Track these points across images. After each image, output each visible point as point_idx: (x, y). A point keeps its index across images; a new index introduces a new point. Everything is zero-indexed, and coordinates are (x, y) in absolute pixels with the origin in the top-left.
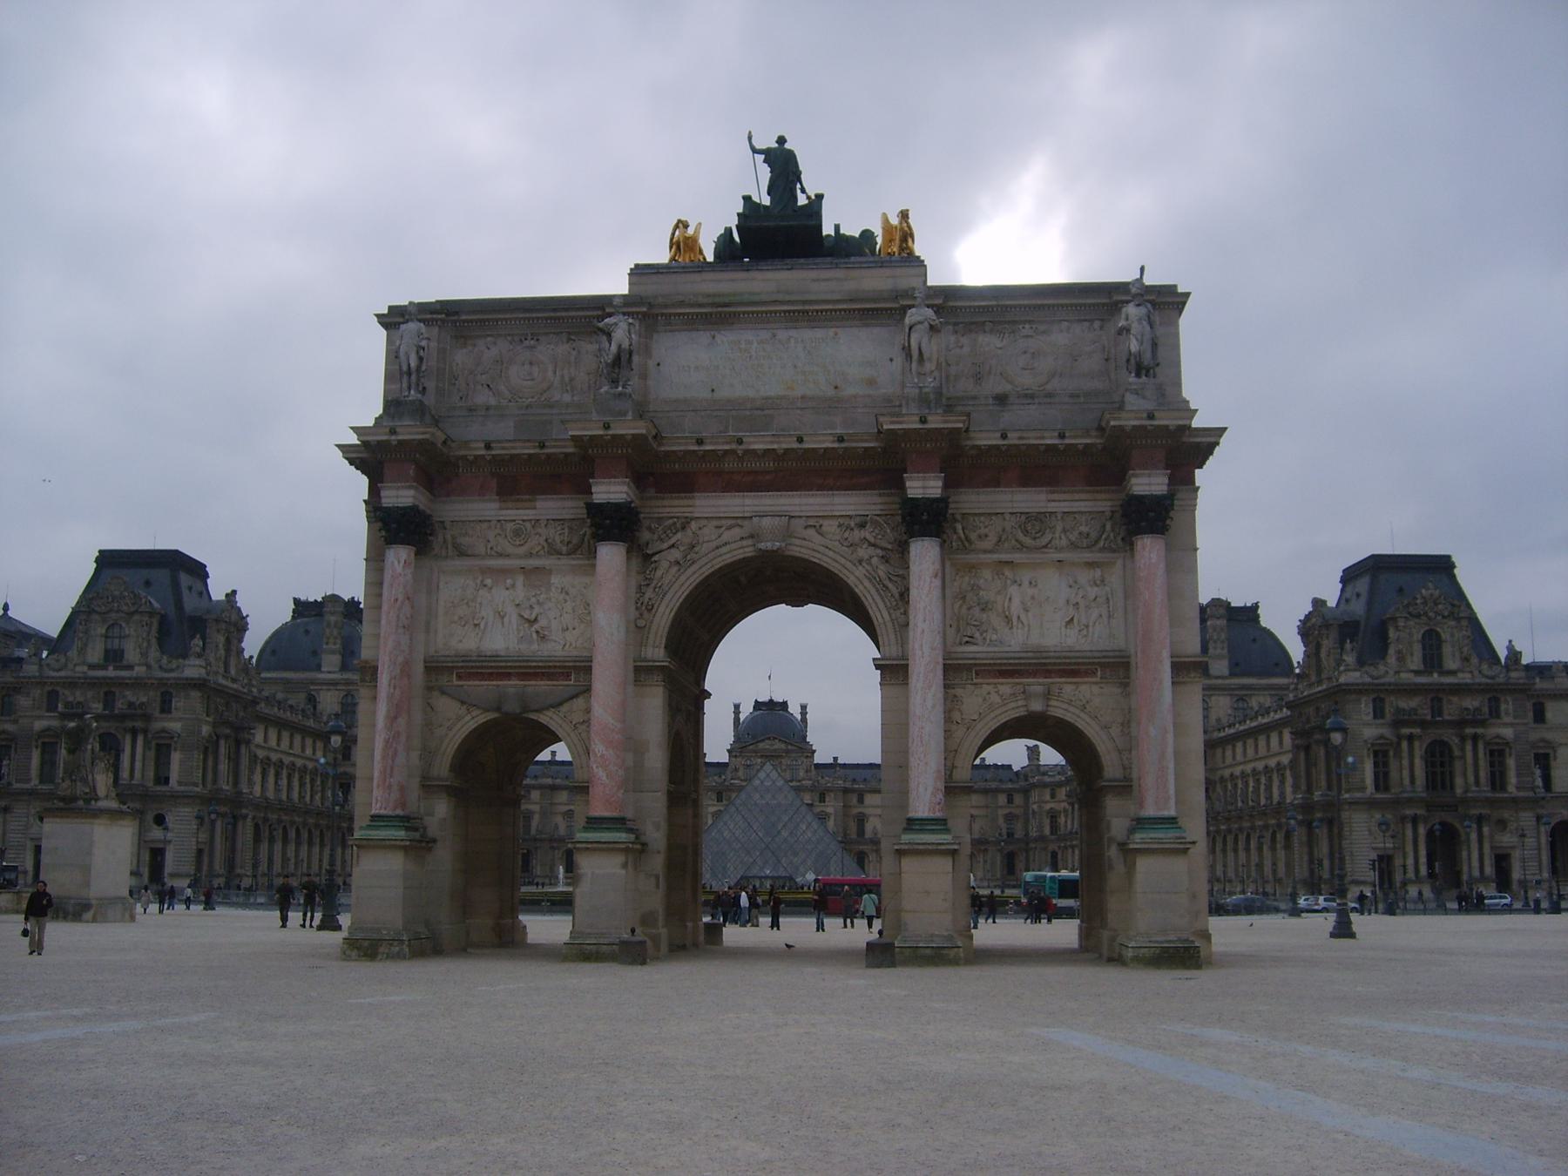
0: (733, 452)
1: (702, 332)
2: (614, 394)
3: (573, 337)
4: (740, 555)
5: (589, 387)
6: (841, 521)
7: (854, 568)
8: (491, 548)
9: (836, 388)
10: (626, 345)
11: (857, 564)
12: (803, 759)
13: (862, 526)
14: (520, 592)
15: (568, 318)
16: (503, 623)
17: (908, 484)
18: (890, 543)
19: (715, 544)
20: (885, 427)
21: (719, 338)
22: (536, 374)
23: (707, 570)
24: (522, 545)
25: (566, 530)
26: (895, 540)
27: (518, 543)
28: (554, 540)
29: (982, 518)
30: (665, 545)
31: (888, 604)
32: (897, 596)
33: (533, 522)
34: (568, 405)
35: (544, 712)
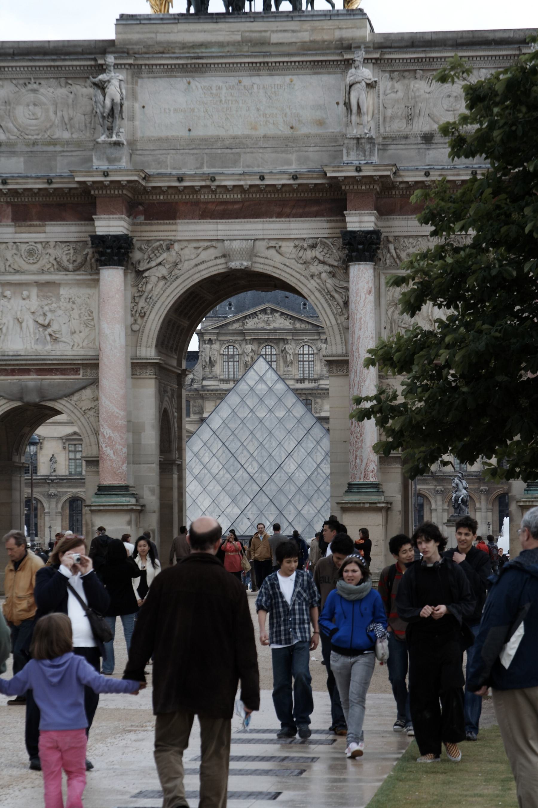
0: (208, 187)
1: (179, 79)
2: (110, 143)
3: (70, 82)
4: (214, 271)
5: (86, 126)
6: (297, 243)
7: (307, 282)
8: (10, 266)
9: (292, 128)
10: (118, 99)
11: (310, 278)
12: (319, 344)
13: (313, 246)
14: (34, 302)
15: (65, 66)
16: (21, 328)
17: (348, 219)
18: (335, 260)
19: (193, 263)
20: (328, 175)
21: (194, 83)
22: (39, 115)
23: (189, 284)
24: (34, 263)
25: (72, 251)
26: (340, 258)
27: (31, 261)
28: (61, 259)
29: (411, 240)
30: (153, 264)
31: (335, 311)
32: (342, 304)
33: (44, 244)
34: (68, 143)
35: (60, 401)
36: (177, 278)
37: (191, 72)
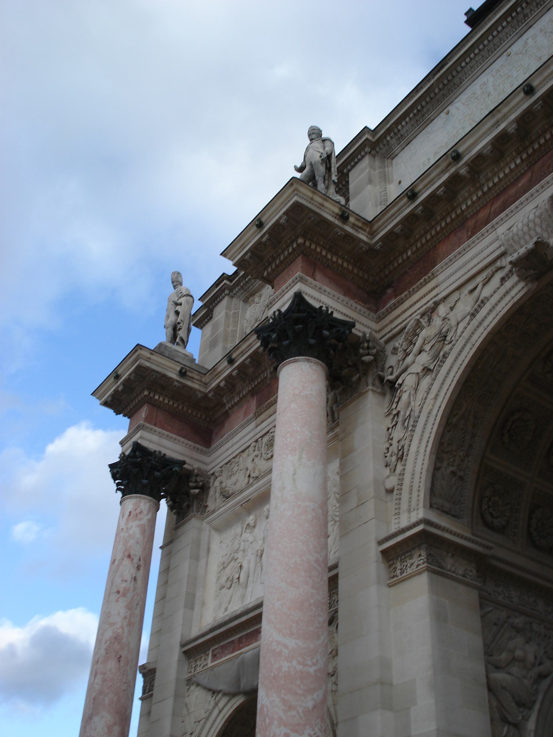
8: (249, 476)
36: (445, 356)
37: (444, 96)
